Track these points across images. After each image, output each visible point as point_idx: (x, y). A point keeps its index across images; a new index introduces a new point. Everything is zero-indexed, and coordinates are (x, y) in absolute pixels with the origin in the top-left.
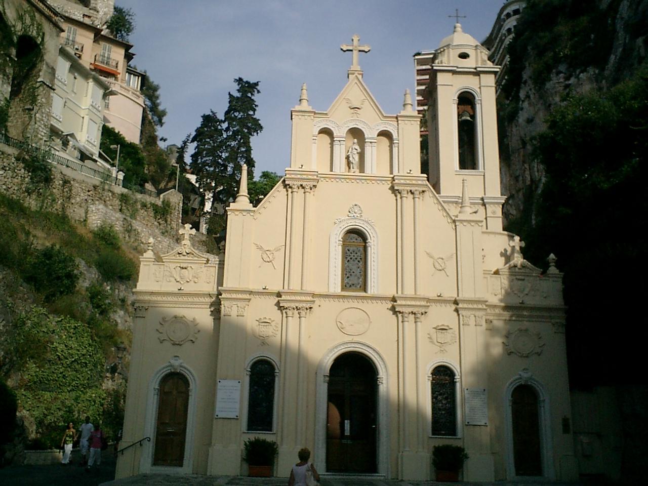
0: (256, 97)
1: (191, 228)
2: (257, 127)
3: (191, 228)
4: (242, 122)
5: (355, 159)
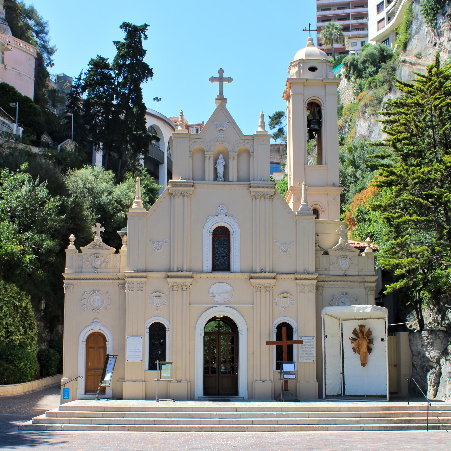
0: (145, 45)
1: (101, 227)
2: (147, 72)
3: (101, 227)
4: (131, 68)
5: (221, 170)
